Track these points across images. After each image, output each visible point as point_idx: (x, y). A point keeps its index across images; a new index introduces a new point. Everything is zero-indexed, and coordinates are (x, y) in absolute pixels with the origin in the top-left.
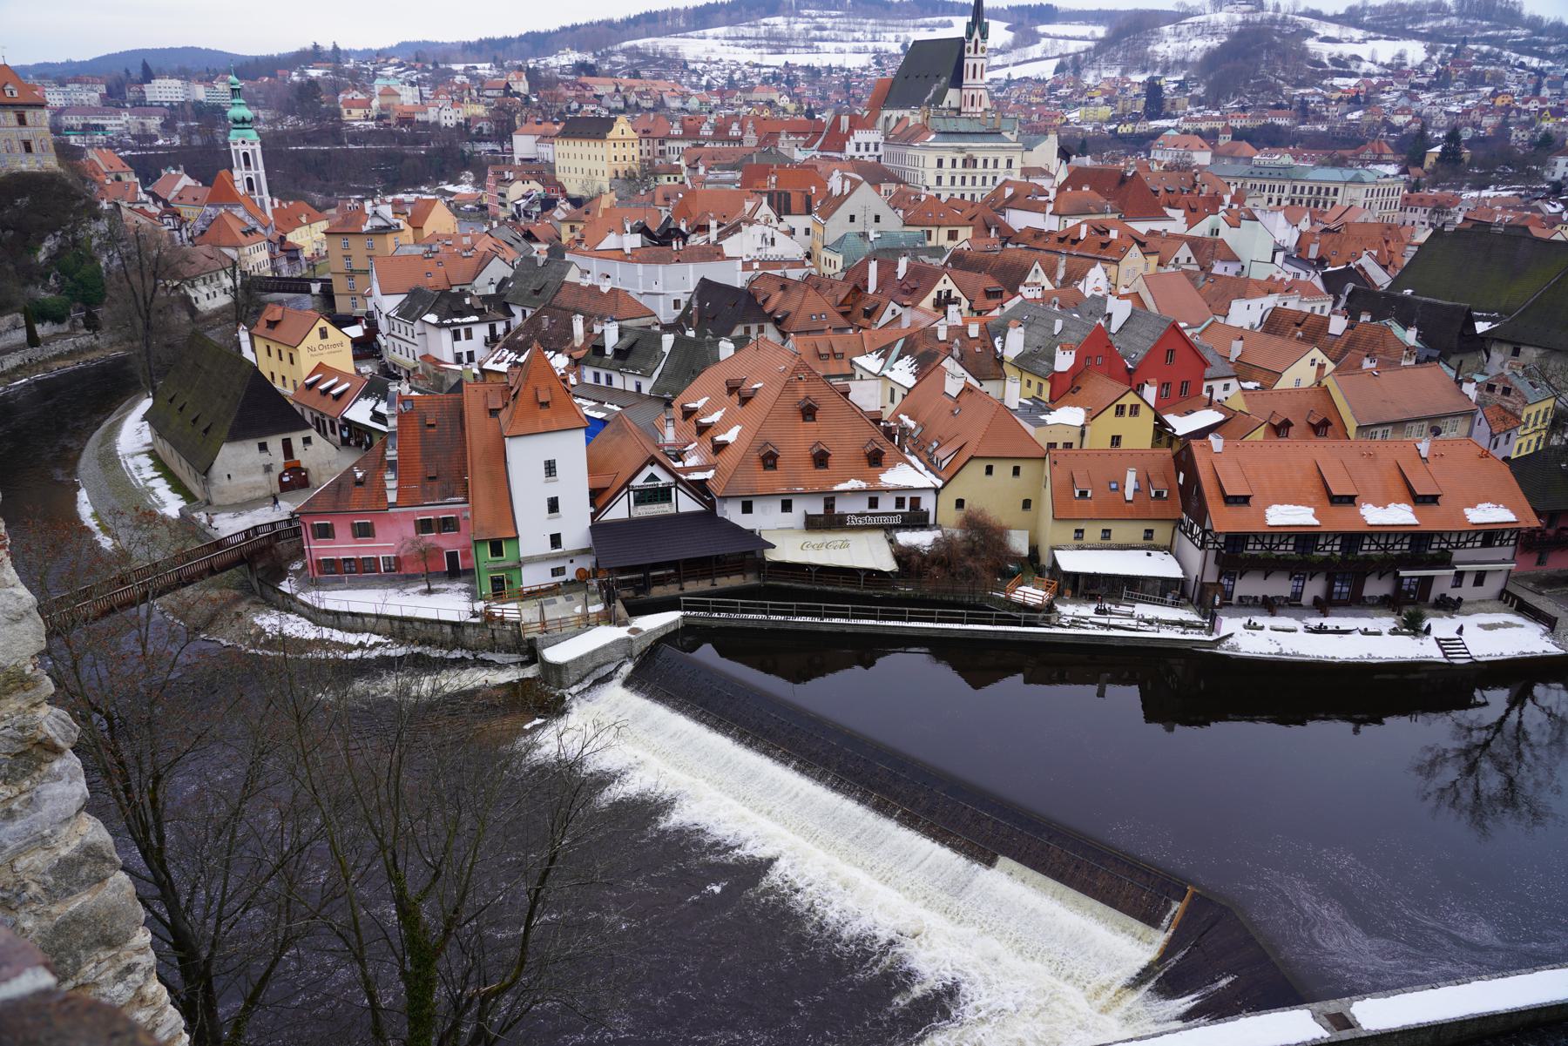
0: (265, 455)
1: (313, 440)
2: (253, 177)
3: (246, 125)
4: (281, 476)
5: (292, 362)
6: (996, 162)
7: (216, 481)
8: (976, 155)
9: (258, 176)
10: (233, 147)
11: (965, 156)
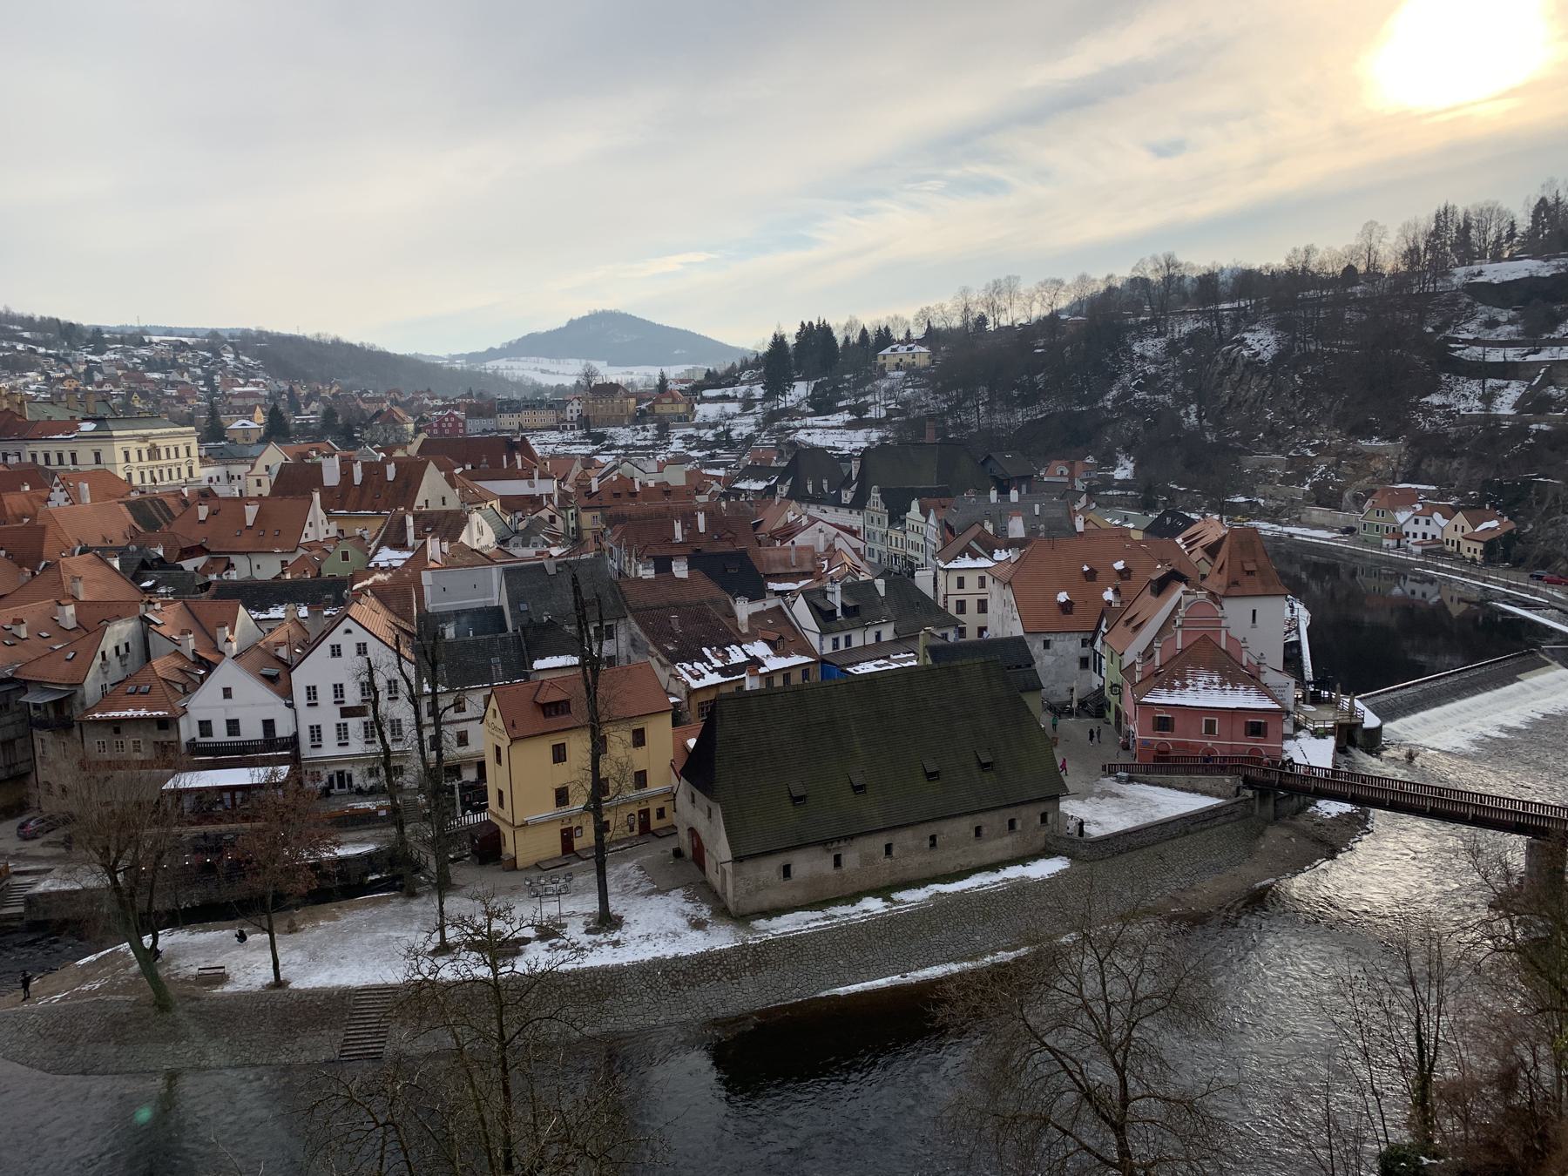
6: (177, 450)
8: (160, 443)
11: (147, 445)
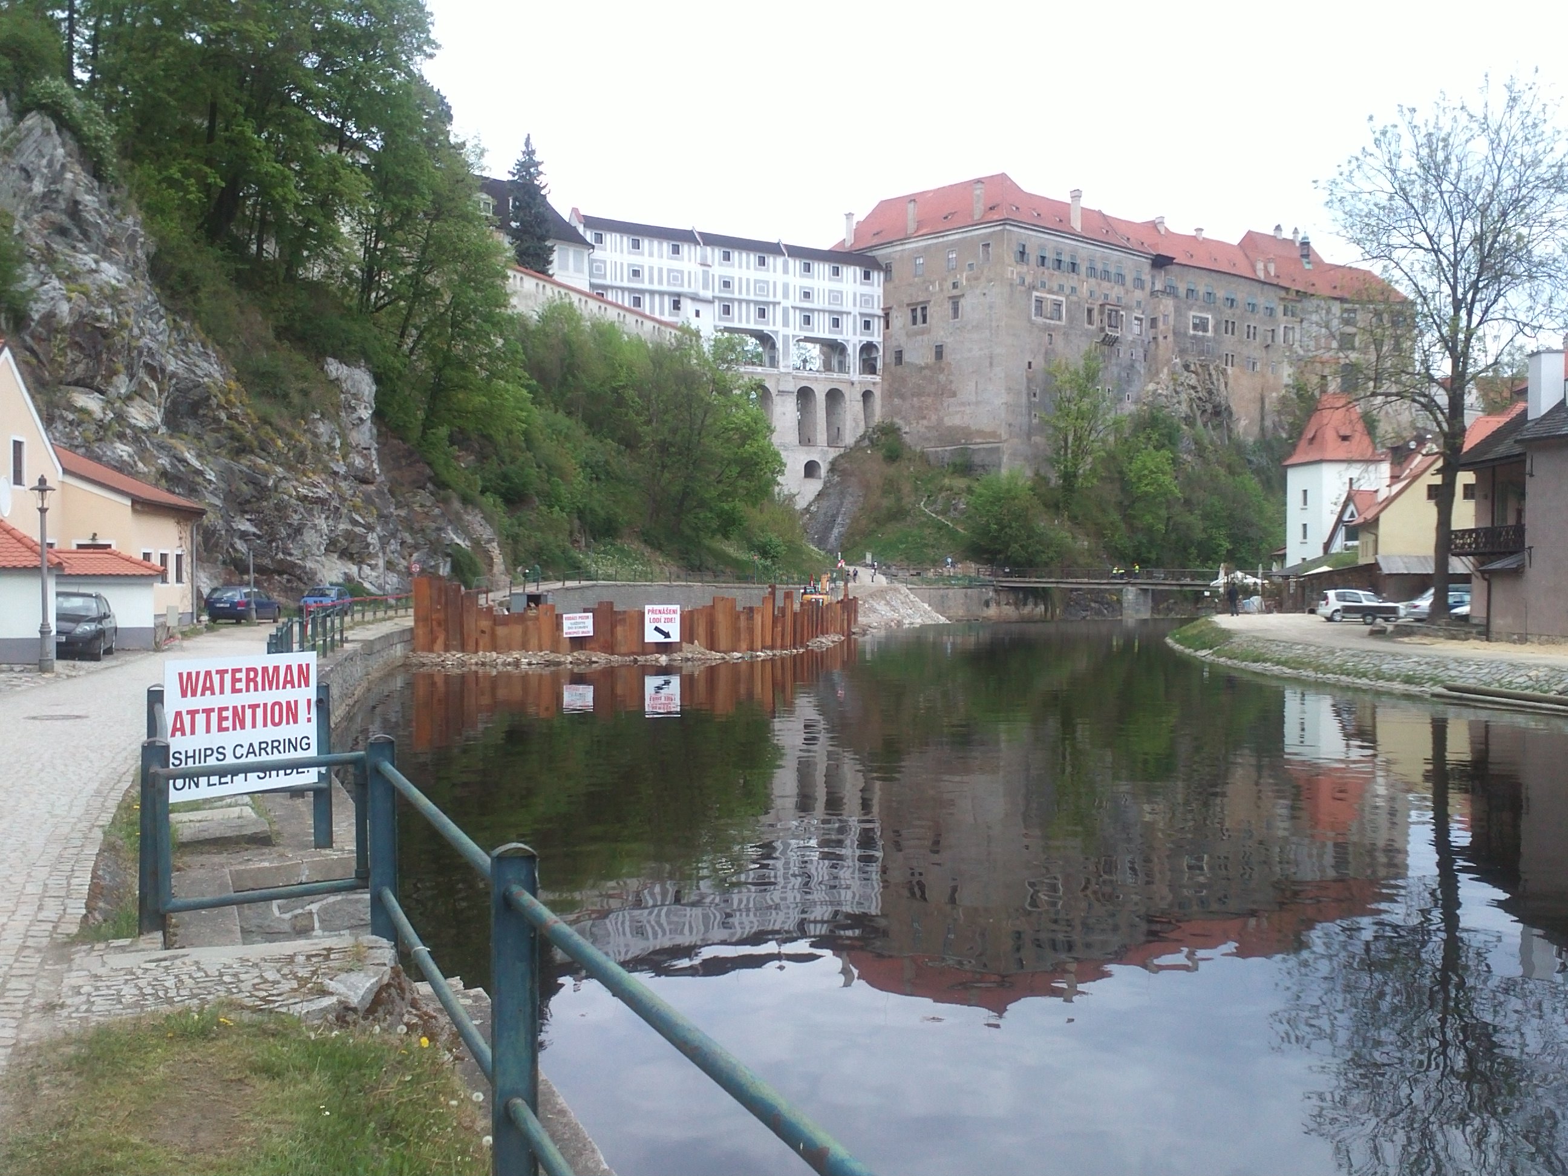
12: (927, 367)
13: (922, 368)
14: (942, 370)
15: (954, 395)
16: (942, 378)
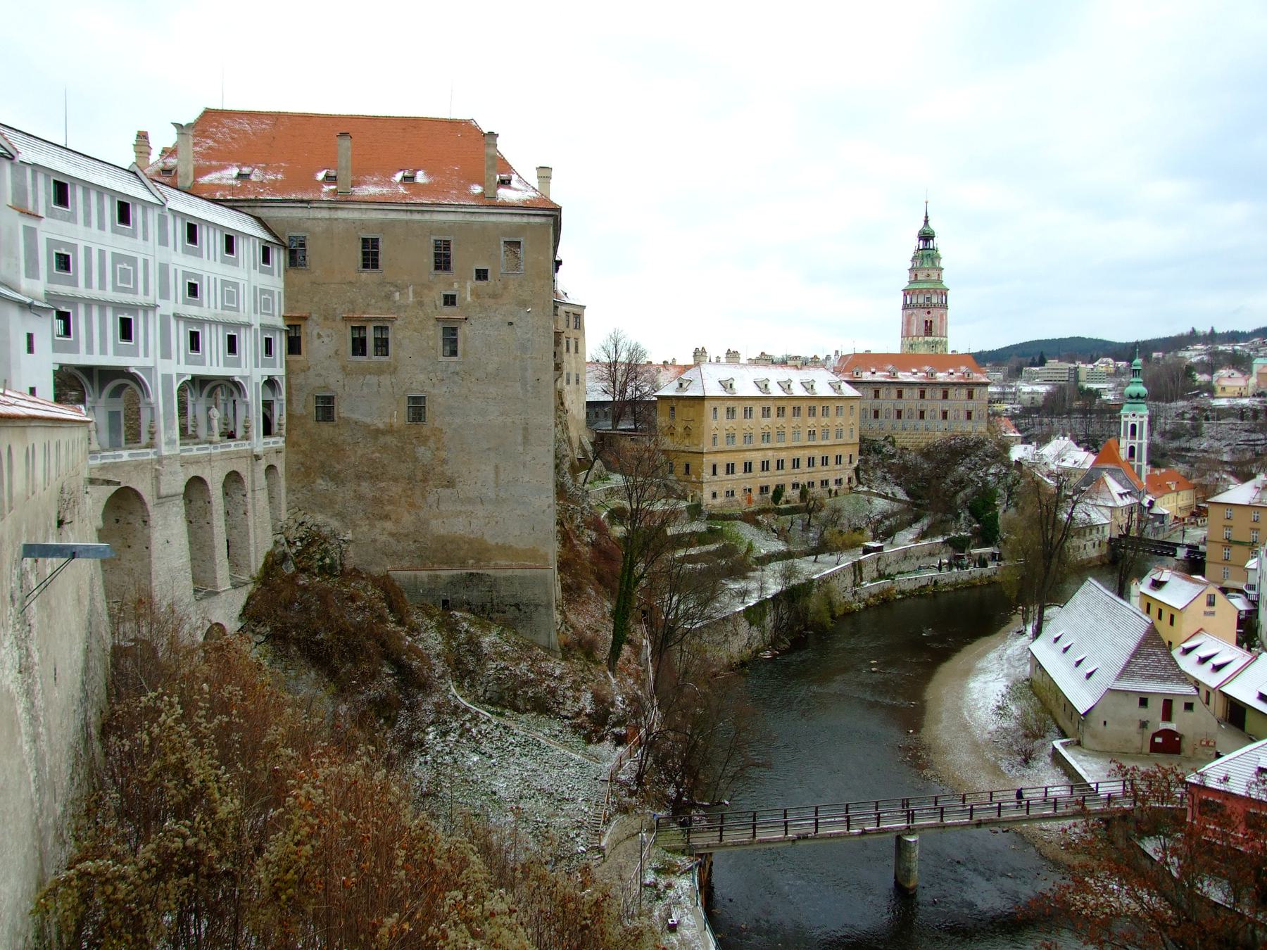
0: (1143, 711)
1: (1195, 707)
2: (1136, 446)
3: (1139, 401)
4: (1155, 735)
5: (1172, 623)
7: (1092, 725)
9: (1140, 445)
10: (1123, 419)
12: (390, 431)
13: (378, 433)
14: (423, 440)
15: (451, 483)
16: (423, 453)
